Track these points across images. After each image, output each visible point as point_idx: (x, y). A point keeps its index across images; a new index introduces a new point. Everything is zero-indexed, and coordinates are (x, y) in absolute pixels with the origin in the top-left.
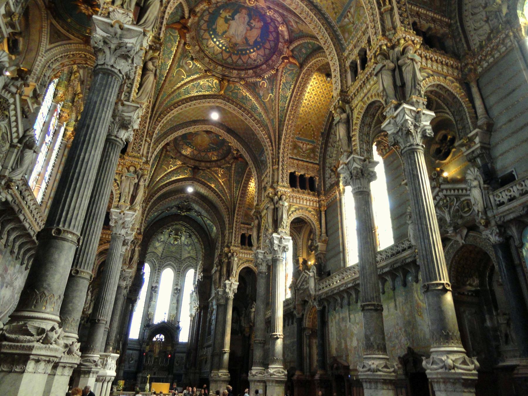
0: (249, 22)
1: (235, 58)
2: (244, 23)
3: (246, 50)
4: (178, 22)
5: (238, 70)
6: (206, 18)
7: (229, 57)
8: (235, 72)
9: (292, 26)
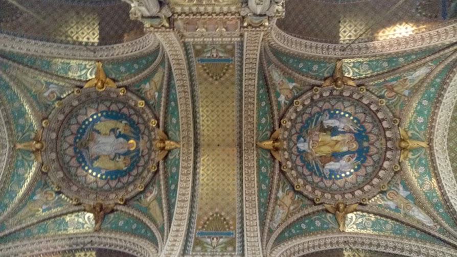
0: (119, 154)
1: (70, 151)
2: (116, 149)
3: (84, 161)
4: (107, 76)
5: (58, 158)
6: (114, 107)
7: (69, 143)
8: (53, 156)
9: (147, 197)
